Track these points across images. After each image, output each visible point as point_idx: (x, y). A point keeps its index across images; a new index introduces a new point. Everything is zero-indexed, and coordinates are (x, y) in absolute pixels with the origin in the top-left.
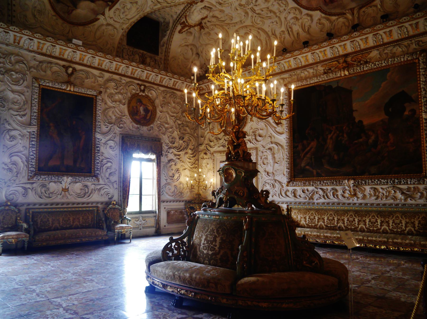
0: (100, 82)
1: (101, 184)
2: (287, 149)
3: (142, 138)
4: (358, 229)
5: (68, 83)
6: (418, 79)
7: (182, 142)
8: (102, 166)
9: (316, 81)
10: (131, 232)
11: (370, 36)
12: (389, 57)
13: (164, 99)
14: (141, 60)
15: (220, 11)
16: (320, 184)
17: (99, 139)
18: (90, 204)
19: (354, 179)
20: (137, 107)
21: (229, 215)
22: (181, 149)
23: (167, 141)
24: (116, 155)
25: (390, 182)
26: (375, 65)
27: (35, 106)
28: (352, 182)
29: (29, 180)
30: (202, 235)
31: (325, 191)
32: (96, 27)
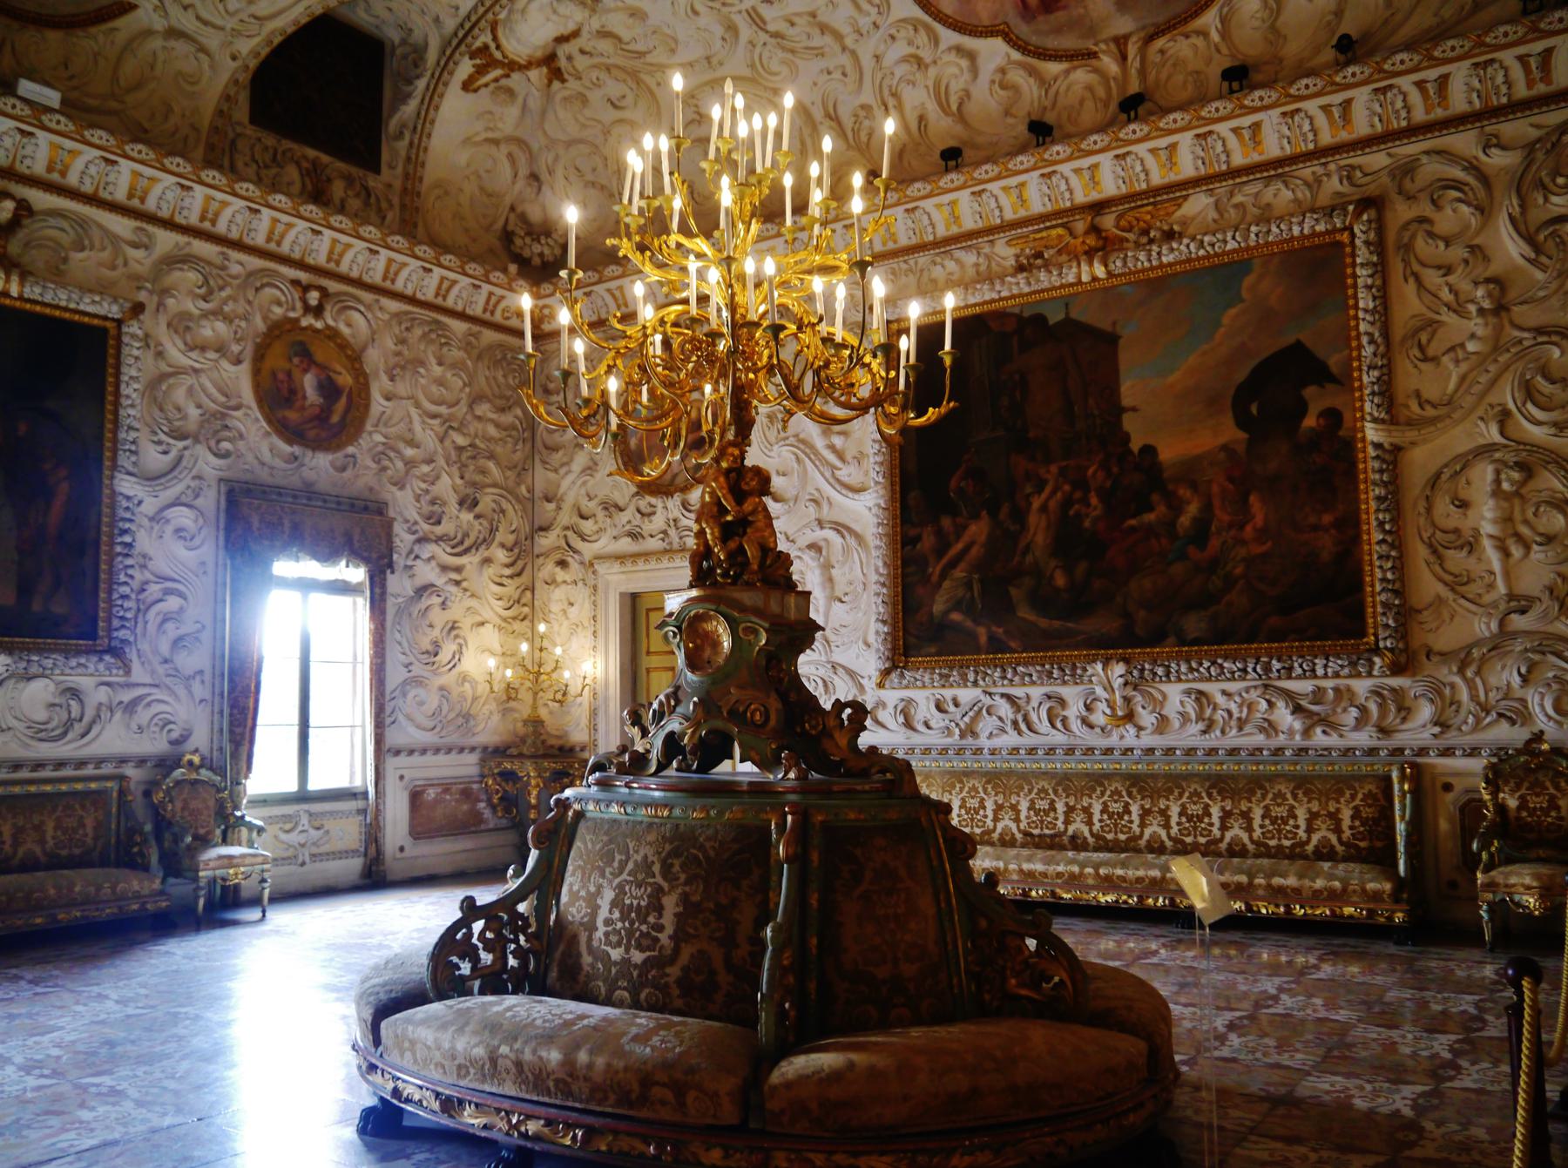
1: (138, 685)
2: (877, 547)
3: (309, 499)
4: (1142, 843)
6: (1351, 302)
7: (470, 516)
9: (987, 297)
10: (266, 875)
11: (1185, 140)
12: (1249, 218)
13: (400, 347)
14: (309, 187)
15: (632, 15)
16: (1004, 678)
17: (128, 498)
18: (91, 766)
19: (1127, 661)
20: (289, 374)
21: (712, 801)
22: (467, 544)
23: (412, 514)
24: (203, 563)
25: (1254, 670)
26: (1201, 245)
28: (1119, 669)
30: (599, 887)
31: (1022, 703)
32: (121, 37)
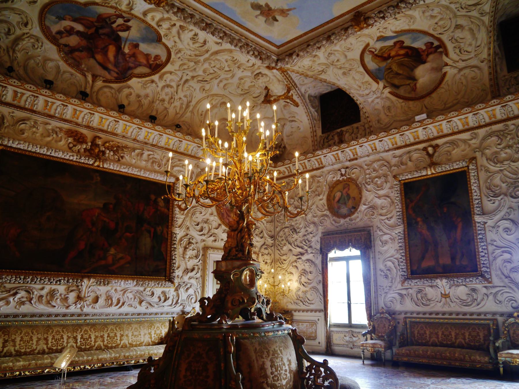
0: (475, 146)
5: (433, 164)
8: (495, 258)
27: (398, 205)
29: (402, 286)
